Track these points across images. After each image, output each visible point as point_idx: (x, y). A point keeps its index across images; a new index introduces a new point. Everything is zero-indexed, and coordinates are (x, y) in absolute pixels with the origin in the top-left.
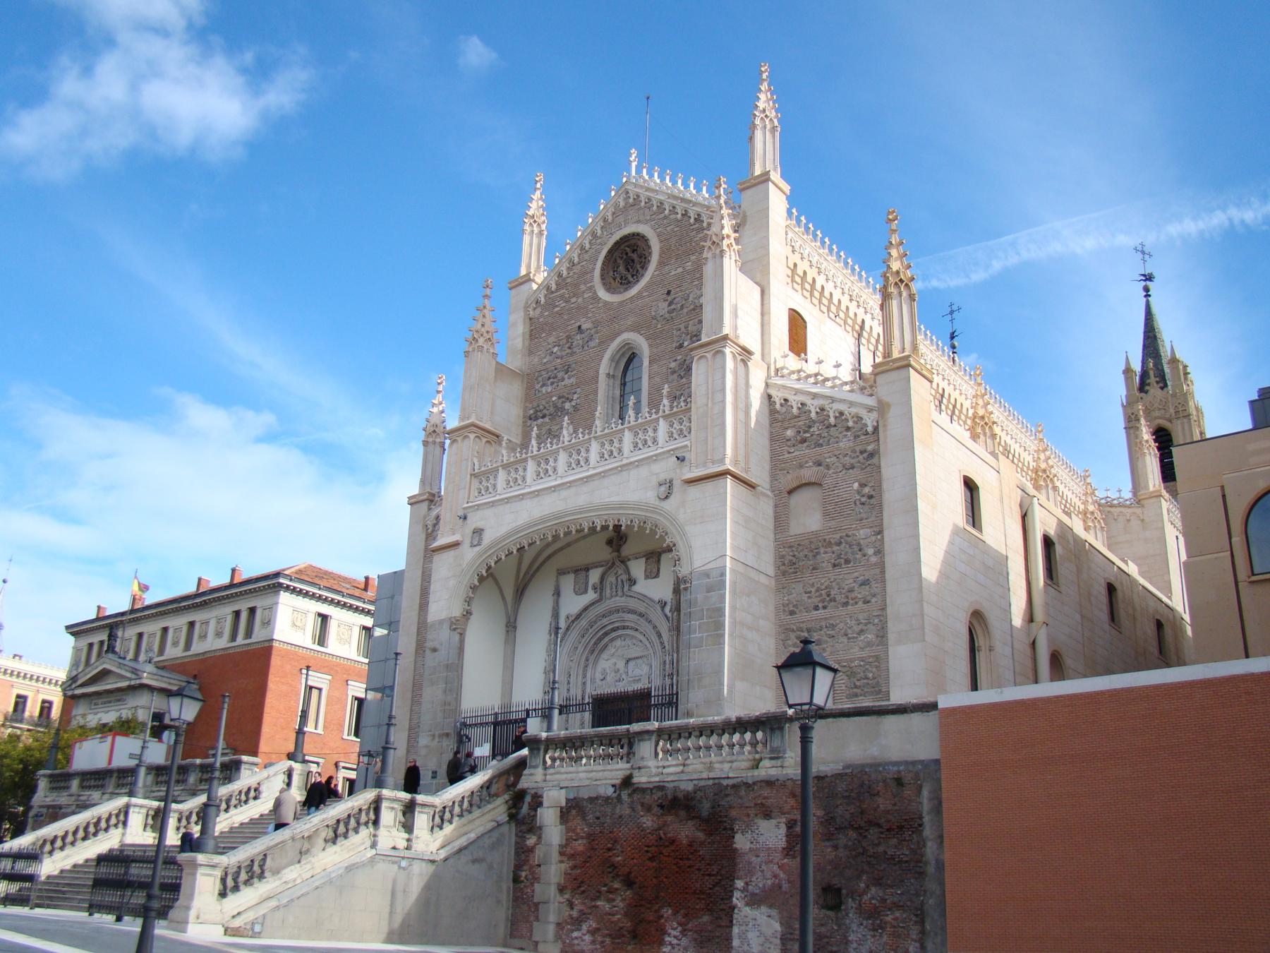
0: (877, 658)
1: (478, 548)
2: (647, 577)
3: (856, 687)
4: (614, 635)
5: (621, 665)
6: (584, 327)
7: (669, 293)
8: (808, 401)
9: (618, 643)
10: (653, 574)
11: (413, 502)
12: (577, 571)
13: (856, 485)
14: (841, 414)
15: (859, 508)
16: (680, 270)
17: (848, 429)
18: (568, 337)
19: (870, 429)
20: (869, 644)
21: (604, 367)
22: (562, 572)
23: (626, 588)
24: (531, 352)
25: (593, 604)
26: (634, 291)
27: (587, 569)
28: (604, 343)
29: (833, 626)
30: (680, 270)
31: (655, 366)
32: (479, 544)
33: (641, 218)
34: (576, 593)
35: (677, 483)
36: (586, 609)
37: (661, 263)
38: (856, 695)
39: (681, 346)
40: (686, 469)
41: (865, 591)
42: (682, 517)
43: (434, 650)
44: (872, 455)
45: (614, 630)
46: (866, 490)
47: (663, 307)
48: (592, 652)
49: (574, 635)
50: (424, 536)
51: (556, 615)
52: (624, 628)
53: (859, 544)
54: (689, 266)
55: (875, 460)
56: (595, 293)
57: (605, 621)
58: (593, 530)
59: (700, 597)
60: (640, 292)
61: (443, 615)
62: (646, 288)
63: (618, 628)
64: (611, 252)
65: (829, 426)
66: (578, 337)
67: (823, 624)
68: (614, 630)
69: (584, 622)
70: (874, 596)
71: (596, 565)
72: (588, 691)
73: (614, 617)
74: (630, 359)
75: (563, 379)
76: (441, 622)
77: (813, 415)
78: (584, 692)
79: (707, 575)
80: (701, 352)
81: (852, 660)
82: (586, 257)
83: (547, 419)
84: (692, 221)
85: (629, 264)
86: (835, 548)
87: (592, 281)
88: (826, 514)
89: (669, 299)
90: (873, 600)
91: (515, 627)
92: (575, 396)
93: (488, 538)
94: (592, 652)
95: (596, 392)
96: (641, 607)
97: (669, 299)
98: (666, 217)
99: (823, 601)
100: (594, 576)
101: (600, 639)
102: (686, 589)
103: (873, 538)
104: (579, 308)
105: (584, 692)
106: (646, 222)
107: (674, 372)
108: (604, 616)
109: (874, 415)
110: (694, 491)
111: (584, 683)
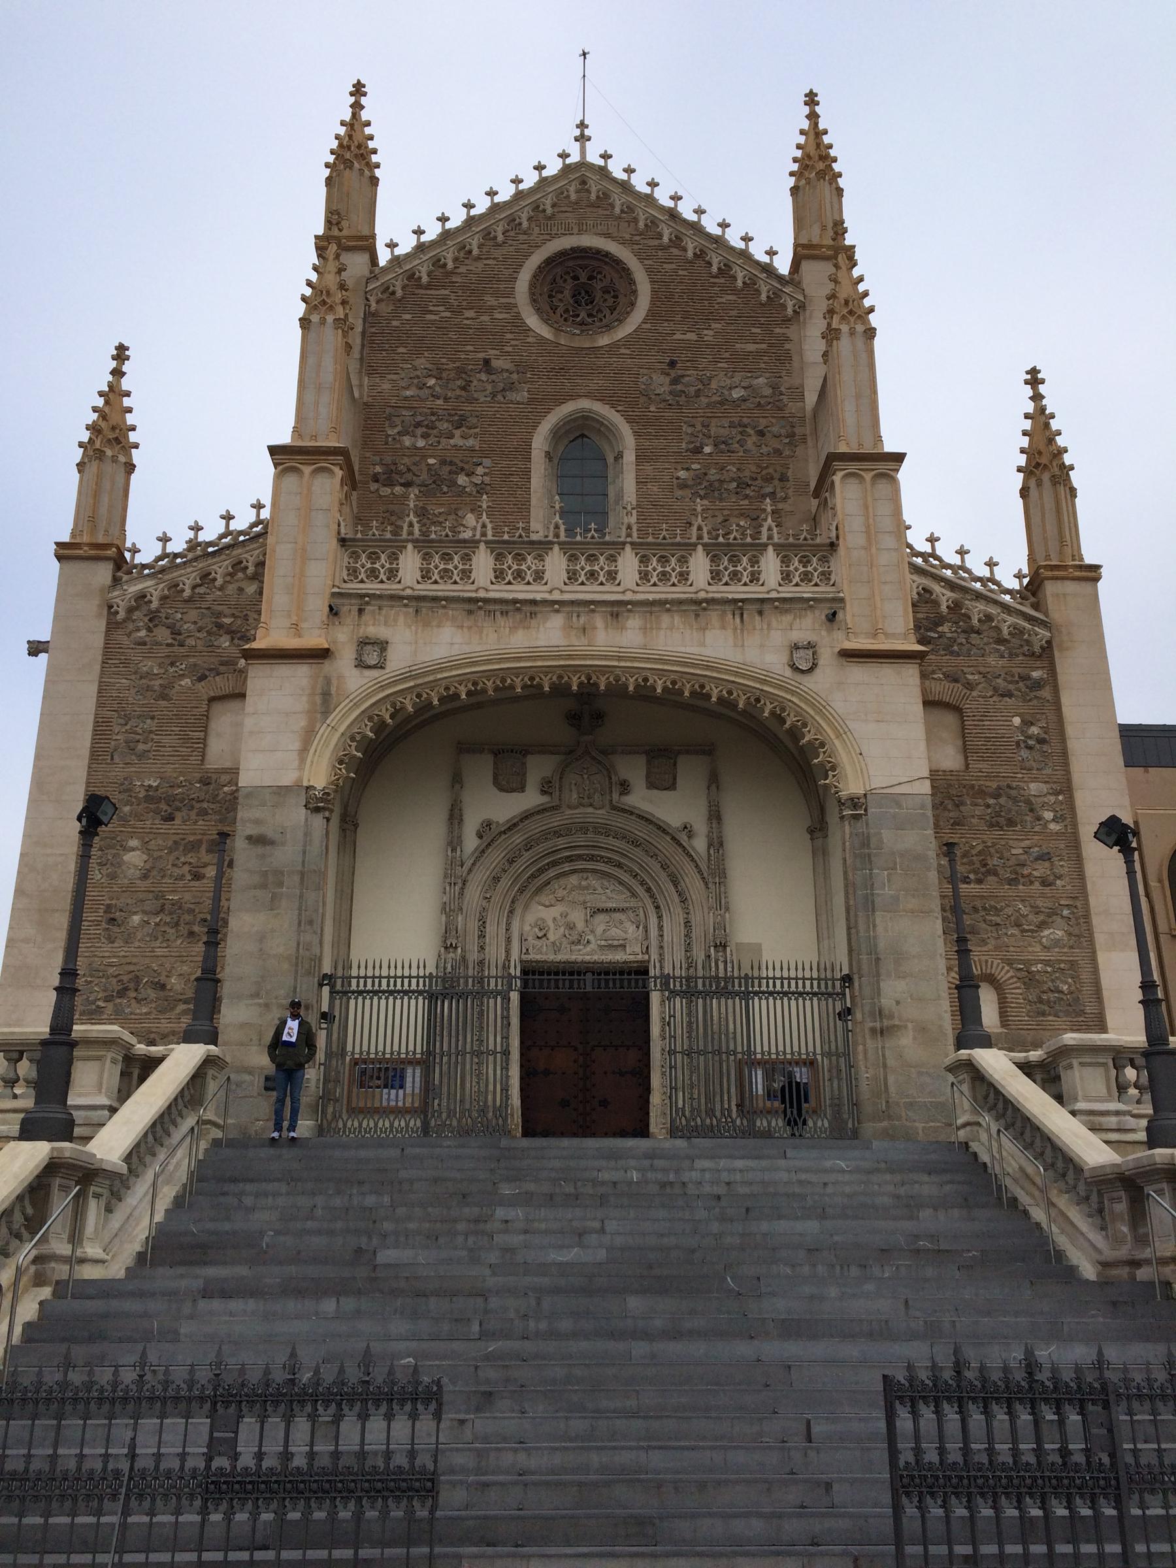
0: (1073, 964)
1: (375, 673)
2: (651, 785)
3: (1041, 1001)
4: (567, 867)
5: (578, 917)
6: (495, 363)
7: (672, 364)
8: (937, 588)
9: (574, 880)
10: (663, 780)
11: (65, 552)
13: (1017, 721)
14: (989, 618)
15: (1024, 753)
16: (692, 336)
17: (1001, 641)
18: (460, 371)
19: (1037, 649)
20: (1057, 943)
21: (540, 442)
22: (464, 748)
23: (615, 796)
24: (369, 368)
25: (545, 810)
26: (604, 341)
27: (525, 751)
28: (541, 404)
29: (998, 911)
30: (692, 336)
31: (648, 468)
32: (380, 666)
34: (502, 789)
35: (826, 656)
36: (526, 816)
37: (653, 314)
38: (1043, 1014)
39: (698, 450)
40: (839, 635)
41: (1041, 870)
42: (840, 704)
43: (258, 840)
44: (1038, 685)
45: (569, 859)
46: (1034, 730)
47: (661, 384)
48: (521, 891)
49: (496, 856)
50: (102, 625)
51: (455, 817)
52: (592, 858)
53: (1028, 802)
54: (708, 335)
55: (1046, 693)
56: (518, 316)
57: (561, 842)
58: (560, 690)
59: (887, 835)
60: (615, 346)
61: (288, 779)
62: (627, 341)
63: (580, 857)
64: (549, 262)
65: (971, 630)
66: (484, 377)
67: (978, 904)
68: (569, 859)
69: (517, 839)
70: (1060, 877)
71: (544, 749)
72: (515, 955)
73: (580, 839)
74: (581, 444)
75: (452, 437)
76: (281, 792)
77: (944, 608)
78: (508, 952)
79: (896, 800)
80: (853, 467)
82: (498, 253)
83: (414, 492)
84: (715, 269)
85: (583, 295)
86: (991, 801)
87: (511, 293)
88: (965, 750)
90: (1058, 882)
91: (356, 826)
92: (480, 470)
93: (400, 658)
94: (521, 891)
95: (527, 474)
96: (641, 831)
97: (673, 373)
99: (975, 872)
100: (538, 768)
101: (541, 871)
102: (856, 817)
103: (1052, 799)
105: (508, 952)
106: (623, 242)
107: (683, 486)
108: (558, 834)
109: (1043, 633)
110: (858, 673)
111: (509, 940)
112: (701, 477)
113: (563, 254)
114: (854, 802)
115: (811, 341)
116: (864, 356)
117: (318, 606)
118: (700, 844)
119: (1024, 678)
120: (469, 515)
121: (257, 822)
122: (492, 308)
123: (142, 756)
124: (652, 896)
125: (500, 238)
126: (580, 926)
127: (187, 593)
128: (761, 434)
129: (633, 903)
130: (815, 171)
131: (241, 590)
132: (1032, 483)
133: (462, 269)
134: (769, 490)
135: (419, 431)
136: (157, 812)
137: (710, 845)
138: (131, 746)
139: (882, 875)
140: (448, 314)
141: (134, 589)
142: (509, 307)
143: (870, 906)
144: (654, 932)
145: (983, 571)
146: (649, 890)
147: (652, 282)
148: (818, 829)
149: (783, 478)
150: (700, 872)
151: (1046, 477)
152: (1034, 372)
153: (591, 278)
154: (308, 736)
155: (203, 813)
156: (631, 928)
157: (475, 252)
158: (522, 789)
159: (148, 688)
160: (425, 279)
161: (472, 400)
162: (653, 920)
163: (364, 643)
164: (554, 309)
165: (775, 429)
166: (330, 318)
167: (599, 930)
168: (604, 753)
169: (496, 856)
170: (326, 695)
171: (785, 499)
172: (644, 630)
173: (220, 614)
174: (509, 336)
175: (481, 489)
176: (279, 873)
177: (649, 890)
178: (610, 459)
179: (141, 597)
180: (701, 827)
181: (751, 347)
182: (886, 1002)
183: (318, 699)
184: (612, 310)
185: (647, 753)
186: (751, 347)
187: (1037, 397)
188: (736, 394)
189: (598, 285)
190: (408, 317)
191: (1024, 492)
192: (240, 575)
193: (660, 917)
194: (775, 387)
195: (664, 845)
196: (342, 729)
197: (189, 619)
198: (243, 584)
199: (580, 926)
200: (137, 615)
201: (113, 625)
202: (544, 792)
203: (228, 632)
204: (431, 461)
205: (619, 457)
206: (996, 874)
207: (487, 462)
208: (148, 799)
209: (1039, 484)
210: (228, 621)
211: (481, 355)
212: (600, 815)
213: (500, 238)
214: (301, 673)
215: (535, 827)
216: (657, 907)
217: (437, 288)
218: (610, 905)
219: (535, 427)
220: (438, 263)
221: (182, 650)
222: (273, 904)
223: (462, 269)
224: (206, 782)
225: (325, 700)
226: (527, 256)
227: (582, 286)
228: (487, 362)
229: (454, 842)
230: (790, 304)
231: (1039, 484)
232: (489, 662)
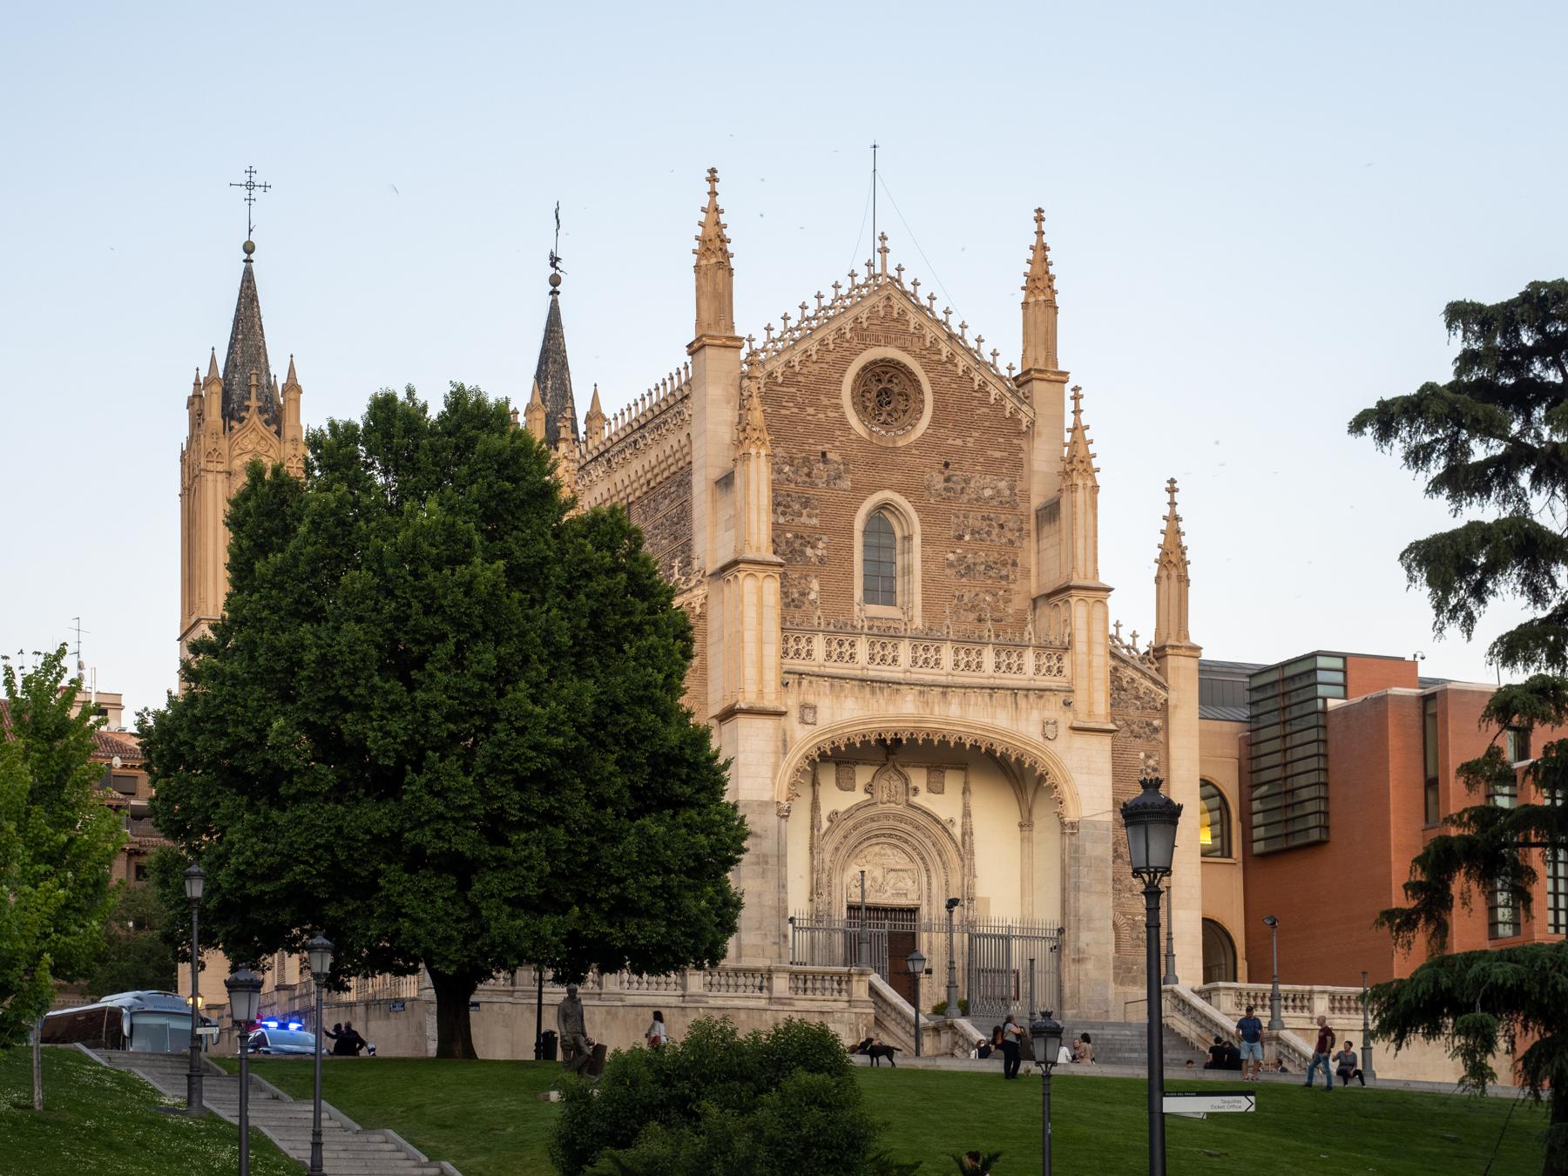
2: (930, 790)
4: (874, 841)
5: (878, 873)
6: (829, 456)
9: (877, 848)
10: (936, 789)
12: (837, 764)
13: (1142, 755)
16: (959, 442)
17: (1138, 698)
18: (806, 460)
30: (959, 442)
33: (908, 344)
35: (1063, 729)
36: (858, 807)
37: (935, 421)
39: (960, 537)
40: (1070, 715)
44: (1156, 730)
46: (1151, 762)
47: (938, 482)
55: (1160, 736)
57: (875, 825)
59: (1088, 846)
60: (908, 447)
61: (766, 797)
64: (864, 368)
66: (821, 466)
73: (886, 823)
75: (801, 515)
79: (1094, 825)
81: (1134, 915)
82: (829, 358)
85: (884, 397)
87: (838, 397)
89: (947, 473)
95: (851, 547)
97: (947, 473)
98: (939, 362)
100: (863, 775)
104: (819, 425)
106: (917, 356)
107: (951, 565)
108: (873, 820)
112: (962, 559)
113: (874, 363)
114: (1073, 825)
115: (1042, 459)
116: (1090, 517)
117: (772, 679)
118: (957, 831)
119: (1149, 724)
122: (826, 407)
124: (925, 863)
125: (831, 347)
126: (880, 880)
128: (1002, 526)
129: (911, 866)
130: (1040, 287)
132: (1164, 573)
133: (805, 371)
134: (1004, 573)
135: (780, 509)
137: (963, 835)
139: (1083, 870)
142: (838, 407)
143: (1077, 889)
144: (925, 886)
145: (1128, 641)
146: (923, 859)
147: (935, 393)
148: (1026, 825)
149: (1014, 564)
151: (1174, 573)
152: (1172, 481)
153: (890, 381)
154: (776, 766)
156: (910, 883)
157: (814, 358)
158: (852, 789)
160: (780, 380)
161: (813, 485)
162: (925, 879)
163: (804, 707)
164: (865, 408)
165: (1011, 524)
166: (763, 452)
169: (840, 833)
170: (785, 741)
171: (1014, 581)
175: (821, 560)
176: (765, 856)
178: (899, 534)
180: (959, 821)
181: (998, 454)
182: (1082, 945)
183: (780, 744)
184: (905, 412)
186: (998, 454)
187: (1173, 504)
188: (988, 493)
189: (896, 390)
191: (1158, 579)
193: (929, 877)
194: (1012, 488)
195: (937, 830)
202: (866, 791)
204: (789, 535)
205: (908, 538)
207: (825, 538)
209: (1169, 577)
211: (819, 448)
212: (900, 809)
213: (831, 347)
214: (768, 724)
215: (861, 815)
217: (788, 386)
219: (856, 511)
220: (788, 364)
222: (763, 875)
223: (805, 371)
225: (785, 745)
226: (849, 362)
227: (886, 390)
228: (824, 454)
230: (1025, 421)
231: (1169, 577)
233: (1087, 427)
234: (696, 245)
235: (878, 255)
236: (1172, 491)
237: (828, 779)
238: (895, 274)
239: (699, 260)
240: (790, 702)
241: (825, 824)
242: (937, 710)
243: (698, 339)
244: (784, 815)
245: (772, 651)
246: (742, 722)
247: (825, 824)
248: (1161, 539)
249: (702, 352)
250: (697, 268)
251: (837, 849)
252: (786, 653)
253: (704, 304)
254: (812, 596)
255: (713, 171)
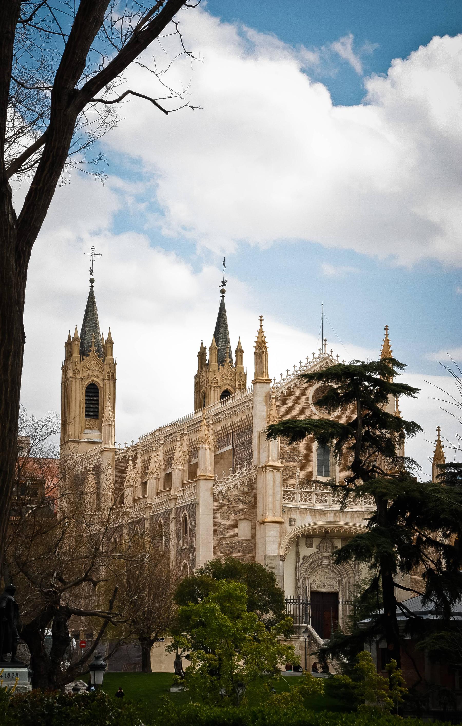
1: (293, 527)
4: (321, 567)
5: (323, 579)
9: (322, 569)
36: (314, 554)
45: (322, 565)
49: (306, 565)
51: (297, 554)
61: (276, 554)
68: (322, 565)
76: (275, 556)
100: (316, 542)
101: (316, 567)
104: (300, 411)
108: (320, 559)
120: (298, 469)
121: (271, 563)
123: (224, 535)
124: (341, 575)
127: (231, 490)
129: (335, 576)
131: (244, 489)
136: (229, 550)
138: (221, 532)
140: (290, 405)
141: (219, 489)
142: (306, 403)
146: (340, 574)
150: (353, 571)
152: (439, 427)
155: (239, 551)
156: (335, 583)
157: (298, 386)
158: (312, 547)
159: (224, 517)
160: (285, 394)
163: (291, 519)
167: (328, 582)
168: (332, 538)
169: (306, 565)
172: (351, 518)
173: (239, 496)
174: (307, 413)
175: (301, 461)
177: (340, 574)
179: (221, 491)
185: (341, 539)
190: (281, 406)
192: (243, 485)
193: (342, 581)
196: (287, 541)
197: (232, 497)
198: (244, 487)
199: (323, 582)
200: (220, 496)
201: (215, 498)
202: (317, 548)
203: (241, 501)
204: (288, 452)
206: (418, 573)
208: (227, 547)
210: (241, 498)
214: (277, 527)
216: (342, 578)
218: (330, 576)
220: (288, 388)
221: (231, 506)
224: (239, 542)
225: (282, 534)
229: (297, 561)
232: (317, 525)
233: (401, 412)
234: (255, 344)
235: (324, 346)
236: (439, 430)
237: (303, 543)
238: (330, 353)
239: (256, 350)
240: (285, 518)
241: (301, 561)
242: (342, 519)
243: (255, 380)
244: (283, 559)
245: (278, 499)
246: (268, 526)
247: (301, 561)
248: (434, 449)
249: (256, 385)
250: (255, 354)
251: (306, 570)
252: (285, 498)
253: (258, 366)
254: (297, 474)
255: (261, 317)
